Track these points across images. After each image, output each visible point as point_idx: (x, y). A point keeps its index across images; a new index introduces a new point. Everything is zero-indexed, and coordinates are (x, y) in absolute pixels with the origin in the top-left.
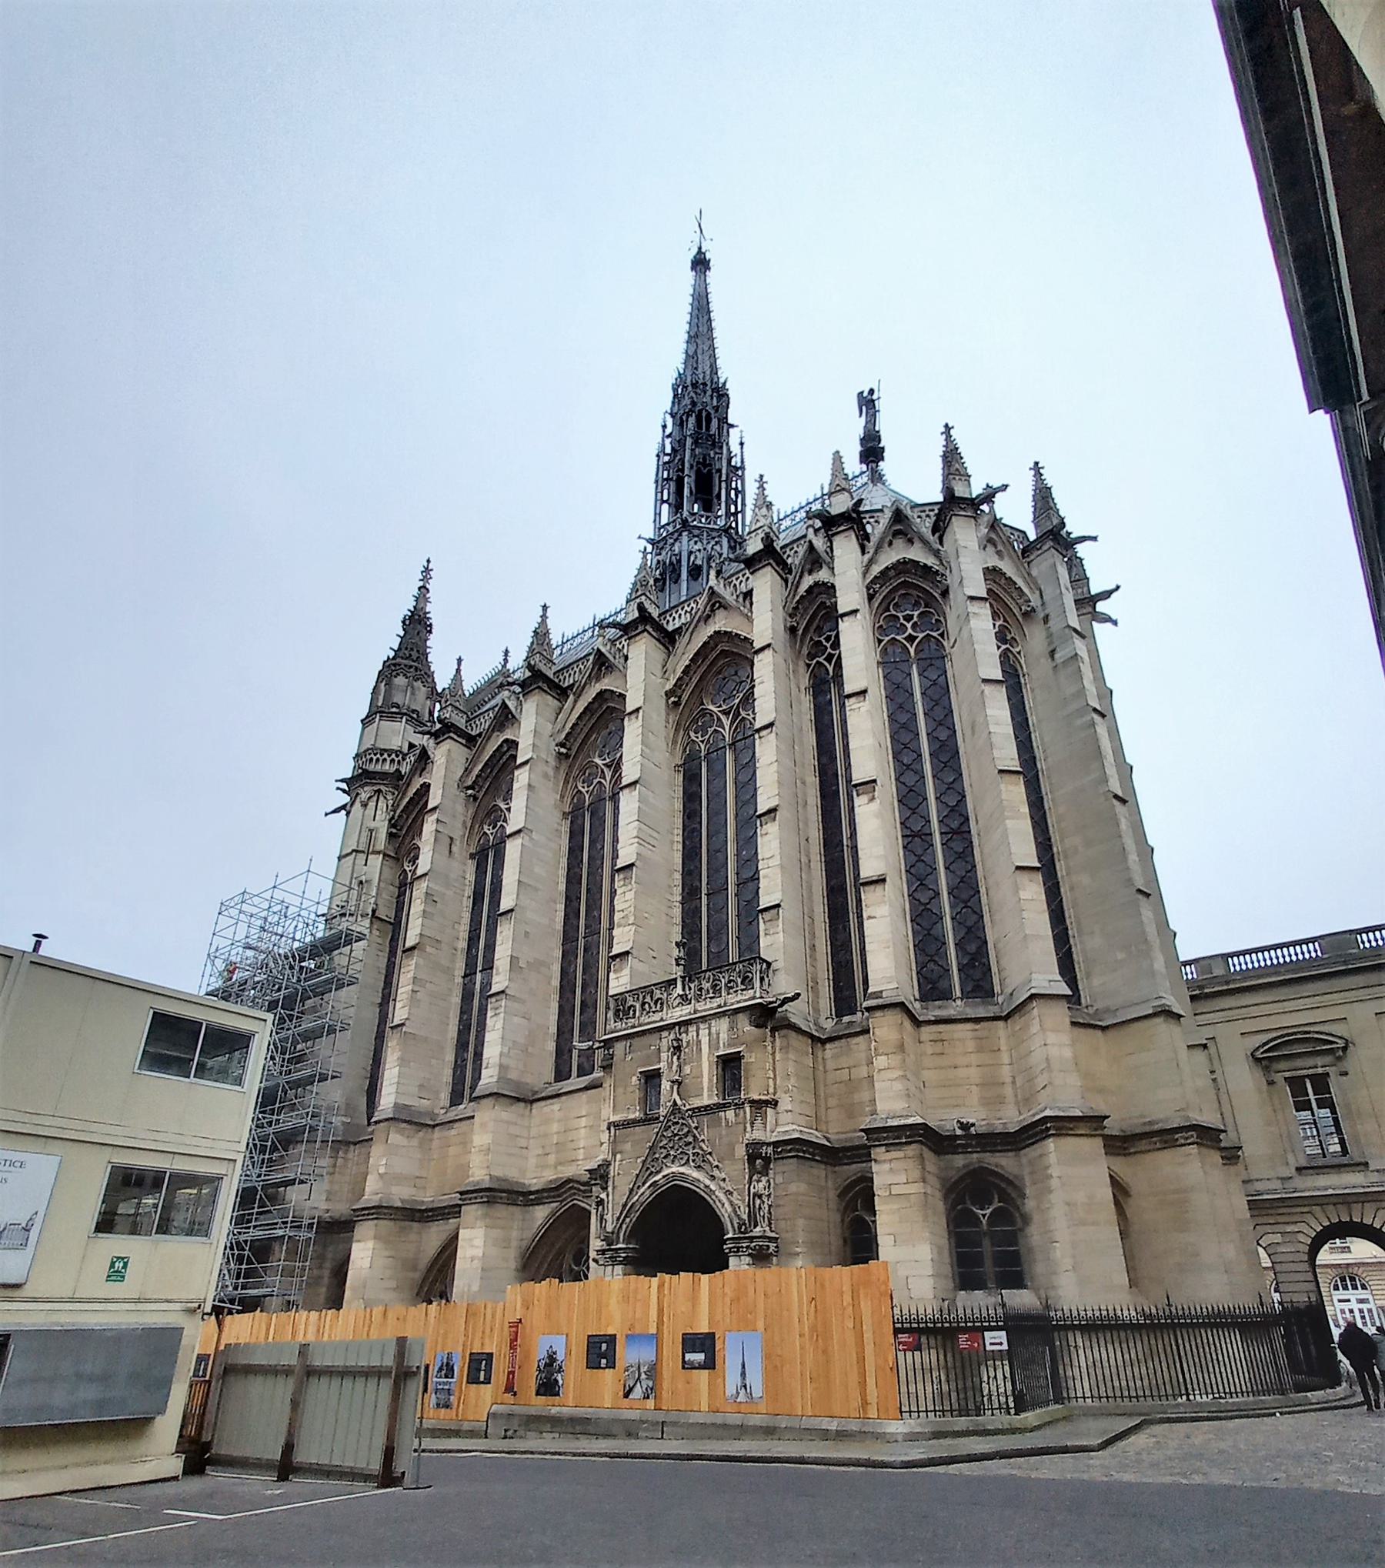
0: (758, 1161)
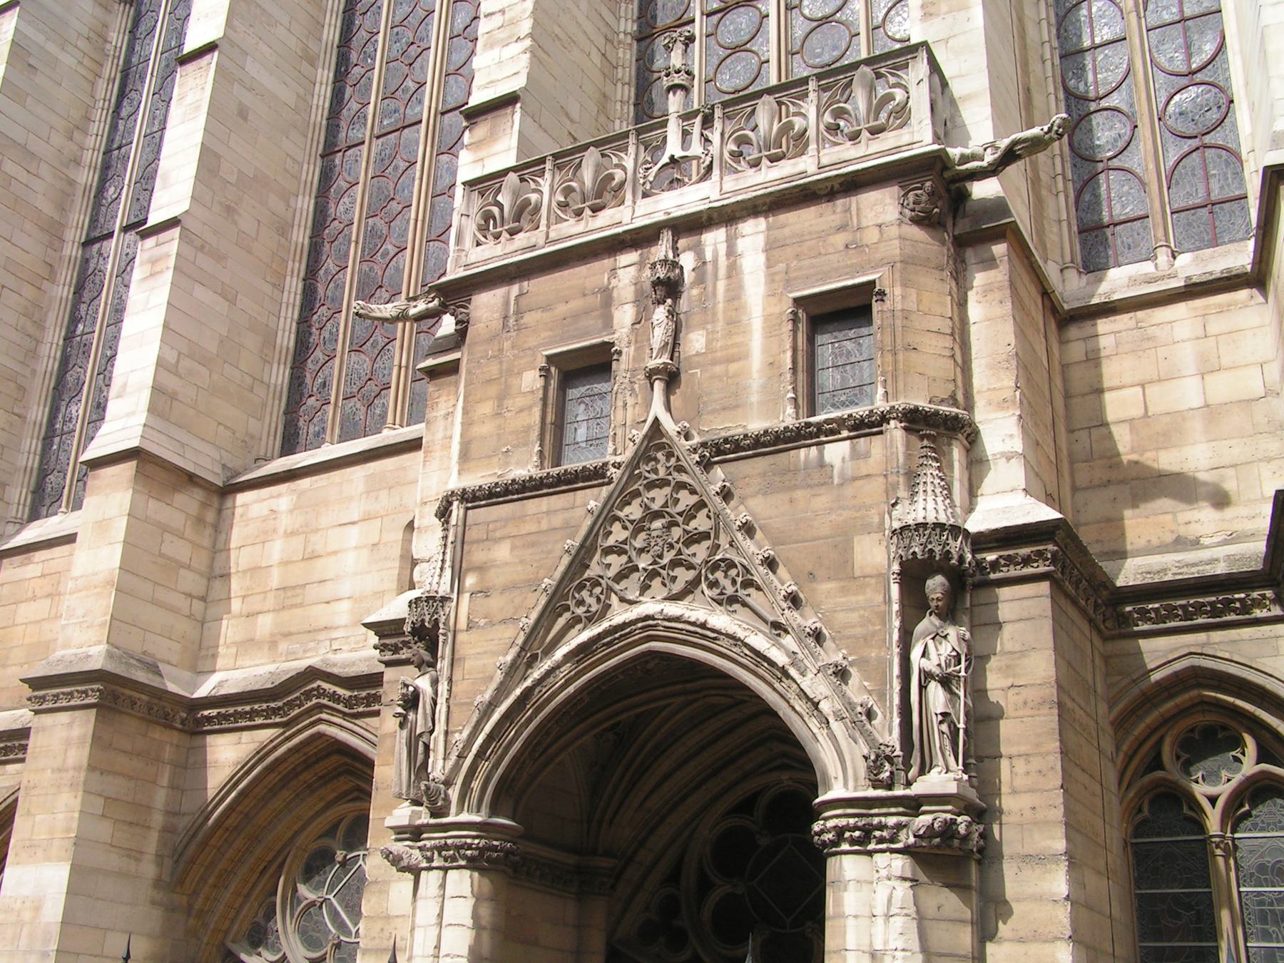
0: (936, 585)
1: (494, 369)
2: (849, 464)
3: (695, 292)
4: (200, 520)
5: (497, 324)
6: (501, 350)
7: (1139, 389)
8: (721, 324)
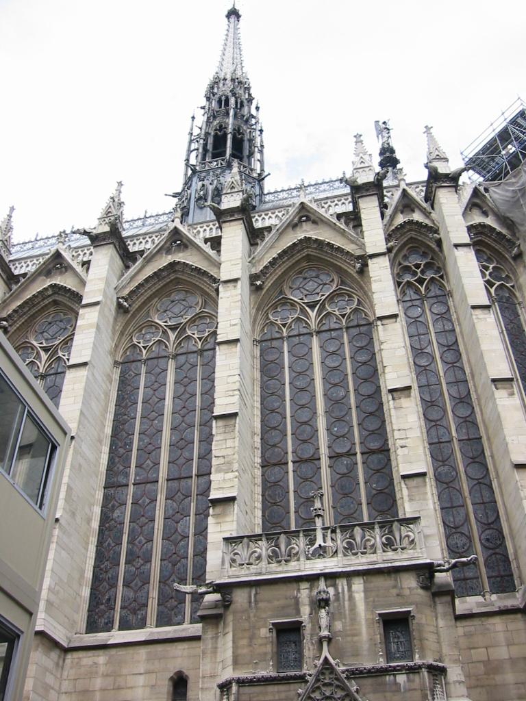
1: (246, 625)
2: (407, 684)
3: (336, 604)
4: (57, 664)
5: (246, 605)
6: (249, 617)
7: (484, 650)
8: (348, 620)
